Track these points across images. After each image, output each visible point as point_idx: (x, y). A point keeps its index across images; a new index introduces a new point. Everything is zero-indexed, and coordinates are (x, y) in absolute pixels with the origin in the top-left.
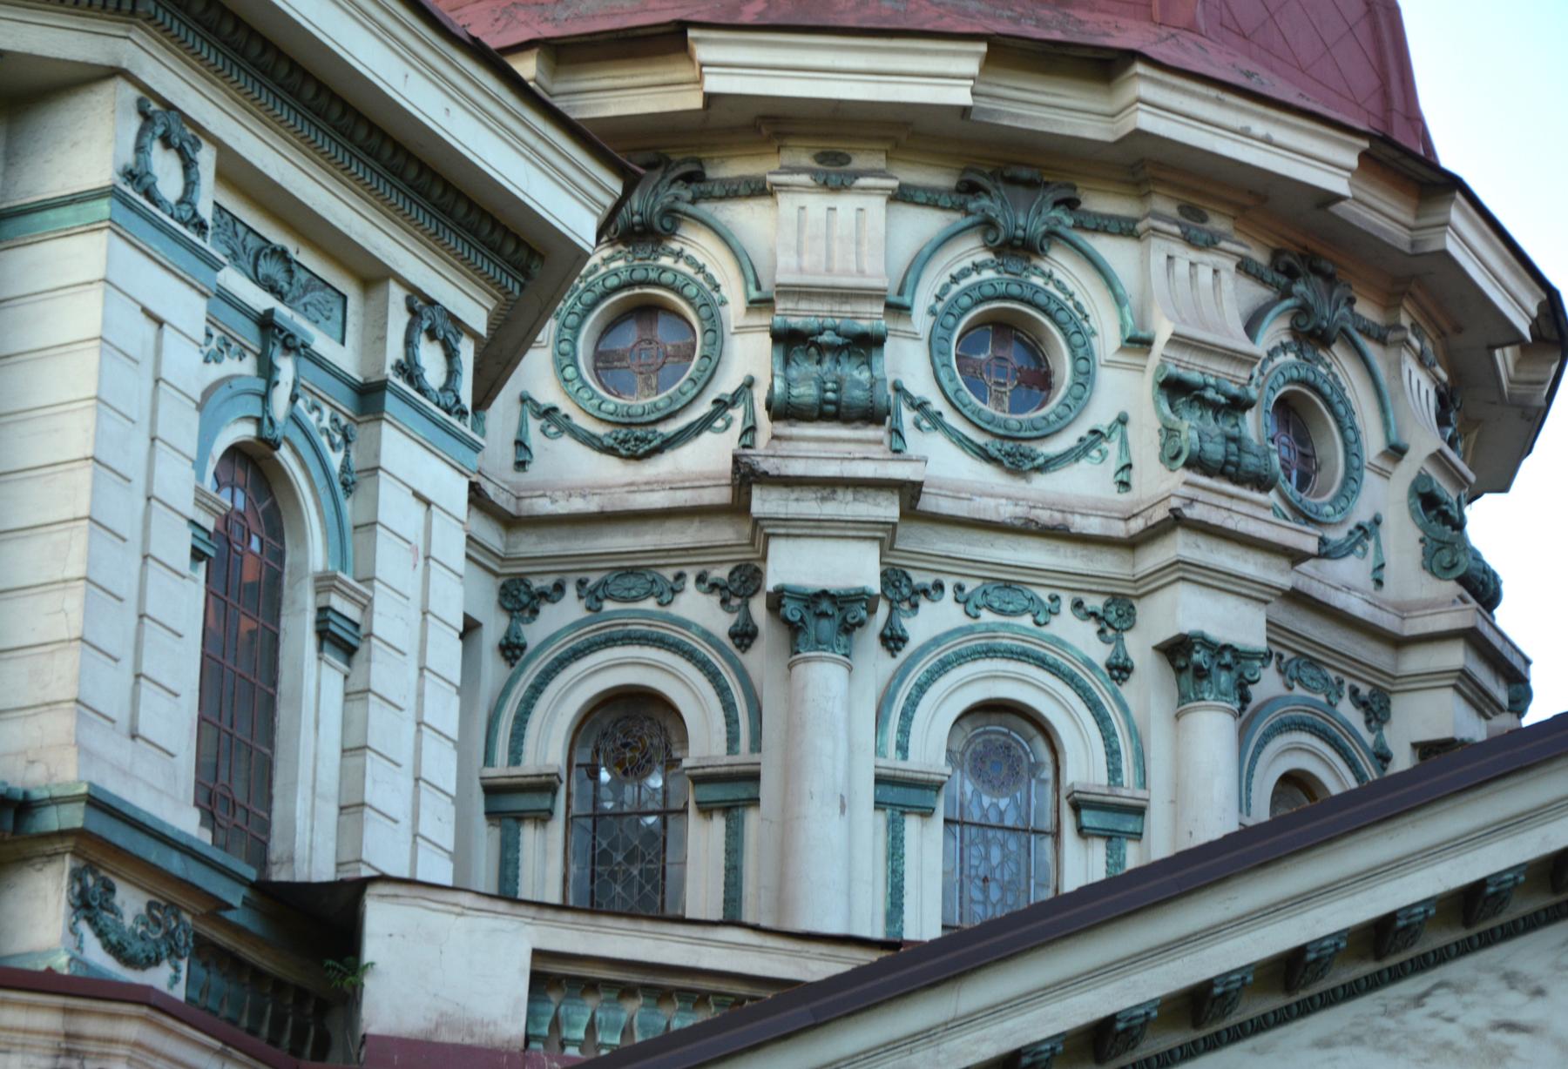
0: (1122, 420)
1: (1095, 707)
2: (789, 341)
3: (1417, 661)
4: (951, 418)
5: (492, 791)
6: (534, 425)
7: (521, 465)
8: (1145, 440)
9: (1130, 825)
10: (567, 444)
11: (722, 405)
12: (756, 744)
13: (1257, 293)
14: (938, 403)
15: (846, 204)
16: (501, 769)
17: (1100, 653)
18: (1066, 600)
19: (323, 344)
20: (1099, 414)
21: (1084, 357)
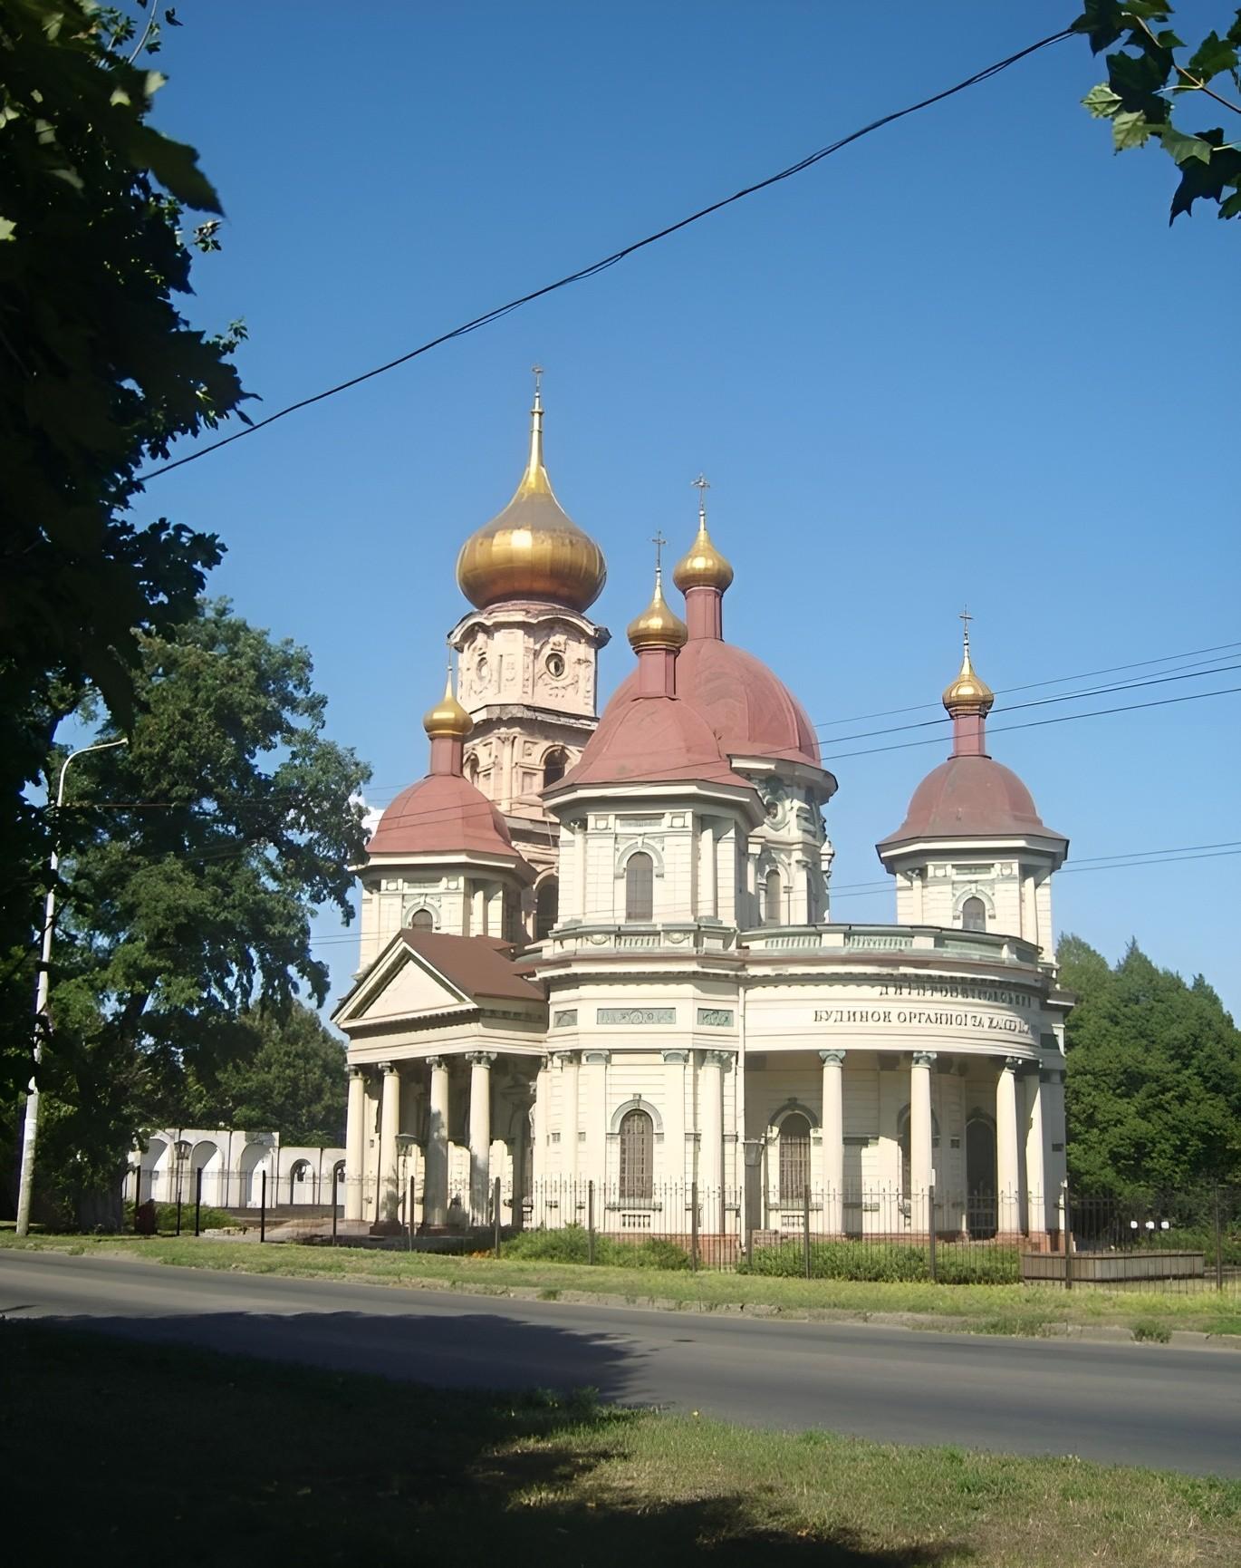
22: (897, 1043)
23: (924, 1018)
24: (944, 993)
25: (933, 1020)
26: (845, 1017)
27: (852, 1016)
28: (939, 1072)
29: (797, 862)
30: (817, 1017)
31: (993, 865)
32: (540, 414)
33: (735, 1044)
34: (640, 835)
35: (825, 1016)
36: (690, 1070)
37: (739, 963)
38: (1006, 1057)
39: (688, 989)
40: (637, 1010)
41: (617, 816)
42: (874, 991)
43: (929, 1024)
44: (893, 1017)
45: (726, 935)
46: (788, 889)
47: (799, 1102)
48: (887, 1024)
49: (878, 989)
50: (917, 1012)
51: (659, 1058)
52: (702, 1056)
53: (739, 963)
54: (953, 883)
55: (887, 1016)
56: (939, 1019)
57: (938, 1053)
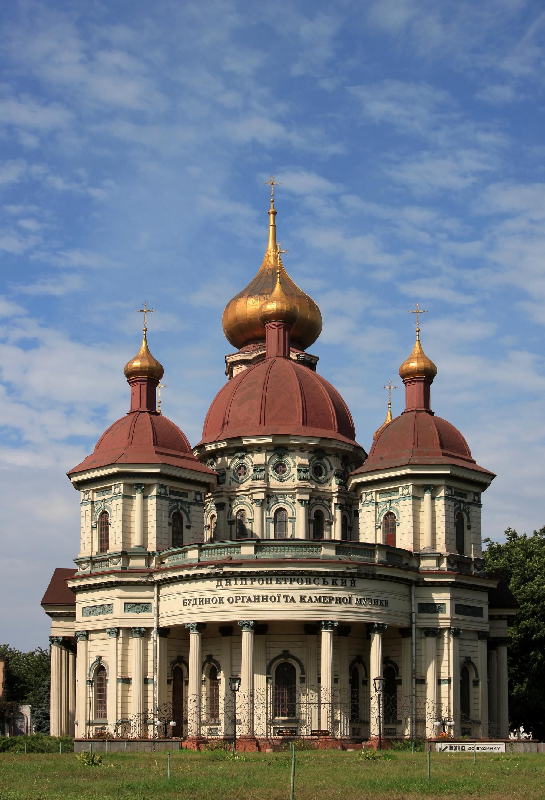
0: (294, 474)
1: (291, 507)
2: (255, 471)
3: (334, 495)
4: (274, 476)
5: (229, 522)
6: (231, 480)
7: (230, 485)
8: (296, 477)
9: (294, 520)
10: (234, 482)
11: (250, 477)
12: (253, 516)
13: (311, 455)
14: (273, 475)
15: (261, 455)
16: (229, 519)
17: (291, 501)
18: (288, 496)
19: (184, 499)
20: (291, 474)
21: (289, 467)
22: (285, 616)
23: (245, 599)
24: (261, 582)
25: (253, 600)
26: (198, 603)
27: (201, 602)
28: (307, 634)
29: (298, 500)
30: (185, 604)
31: (398, 488)
32: (275, 213)
33: (152, 624)
34: (102, 501)
35: (188, 602)
36: (120, 641)
37: (148, 574)
38: (320, 621)
39: (117, 592)
40: (97, 607)
41: (94, 491)
42: (211, 584)
43: (249, 603)
44: (225, 600)
45: (149, 557)
46: (293, 520)
47: (213, 658)
48: (221, 605)
49: (215, 583)
50: (241, 595)
51: (105, 635)
52: (129, 631)
53: (148, 574)
54: (377, 503)
55: (221, 600)
56: (257, 599)
57: (255, 621)
